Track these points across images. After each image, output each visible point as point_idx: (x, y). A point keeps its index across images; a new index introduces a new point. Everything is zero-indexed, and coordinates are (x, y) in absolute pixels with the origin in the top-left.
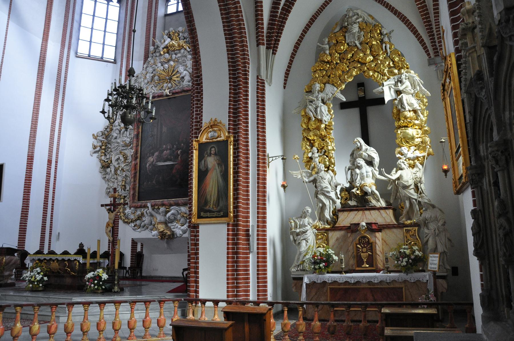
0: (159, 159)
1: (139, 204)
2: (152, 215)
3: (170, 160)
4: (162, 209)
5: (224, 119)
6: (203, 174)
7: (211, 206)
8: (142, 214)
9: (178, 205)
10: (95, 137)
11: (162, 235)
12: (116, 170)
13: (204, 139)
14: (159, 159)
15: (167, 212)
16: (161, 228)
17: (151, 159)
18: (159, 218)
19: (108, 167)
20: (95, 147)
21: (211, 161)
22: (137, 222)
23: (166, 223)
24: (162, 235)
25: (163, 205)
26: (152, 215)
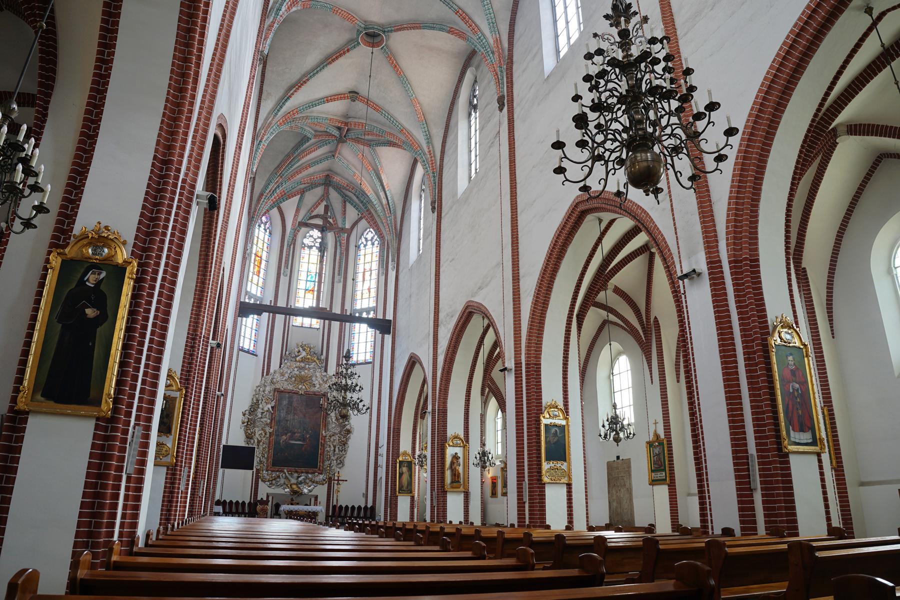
0: (291, 438)
1: (277, 468)
2: (286, 478)
3: (299, 440)
4: (296, 475)
5: (410, 451)
6: (401, 474)
7: (404, 488)
8: (279, 477)
9: (307, 473)
10: (244, 415)
11: (294, 492)
12: (259, 442)
13: (401, 459)
14: (291, 438)
15: (298, 477)
16: (294, 486)
17: (284, 437)
18: (293, 481)
19: (251, 438)
20: (243, 423)
21: (405, 469)
22: (272, 482)
23: (296, 484)
24: (294, 492)
25: (297, 472)
26: (286, 478)
